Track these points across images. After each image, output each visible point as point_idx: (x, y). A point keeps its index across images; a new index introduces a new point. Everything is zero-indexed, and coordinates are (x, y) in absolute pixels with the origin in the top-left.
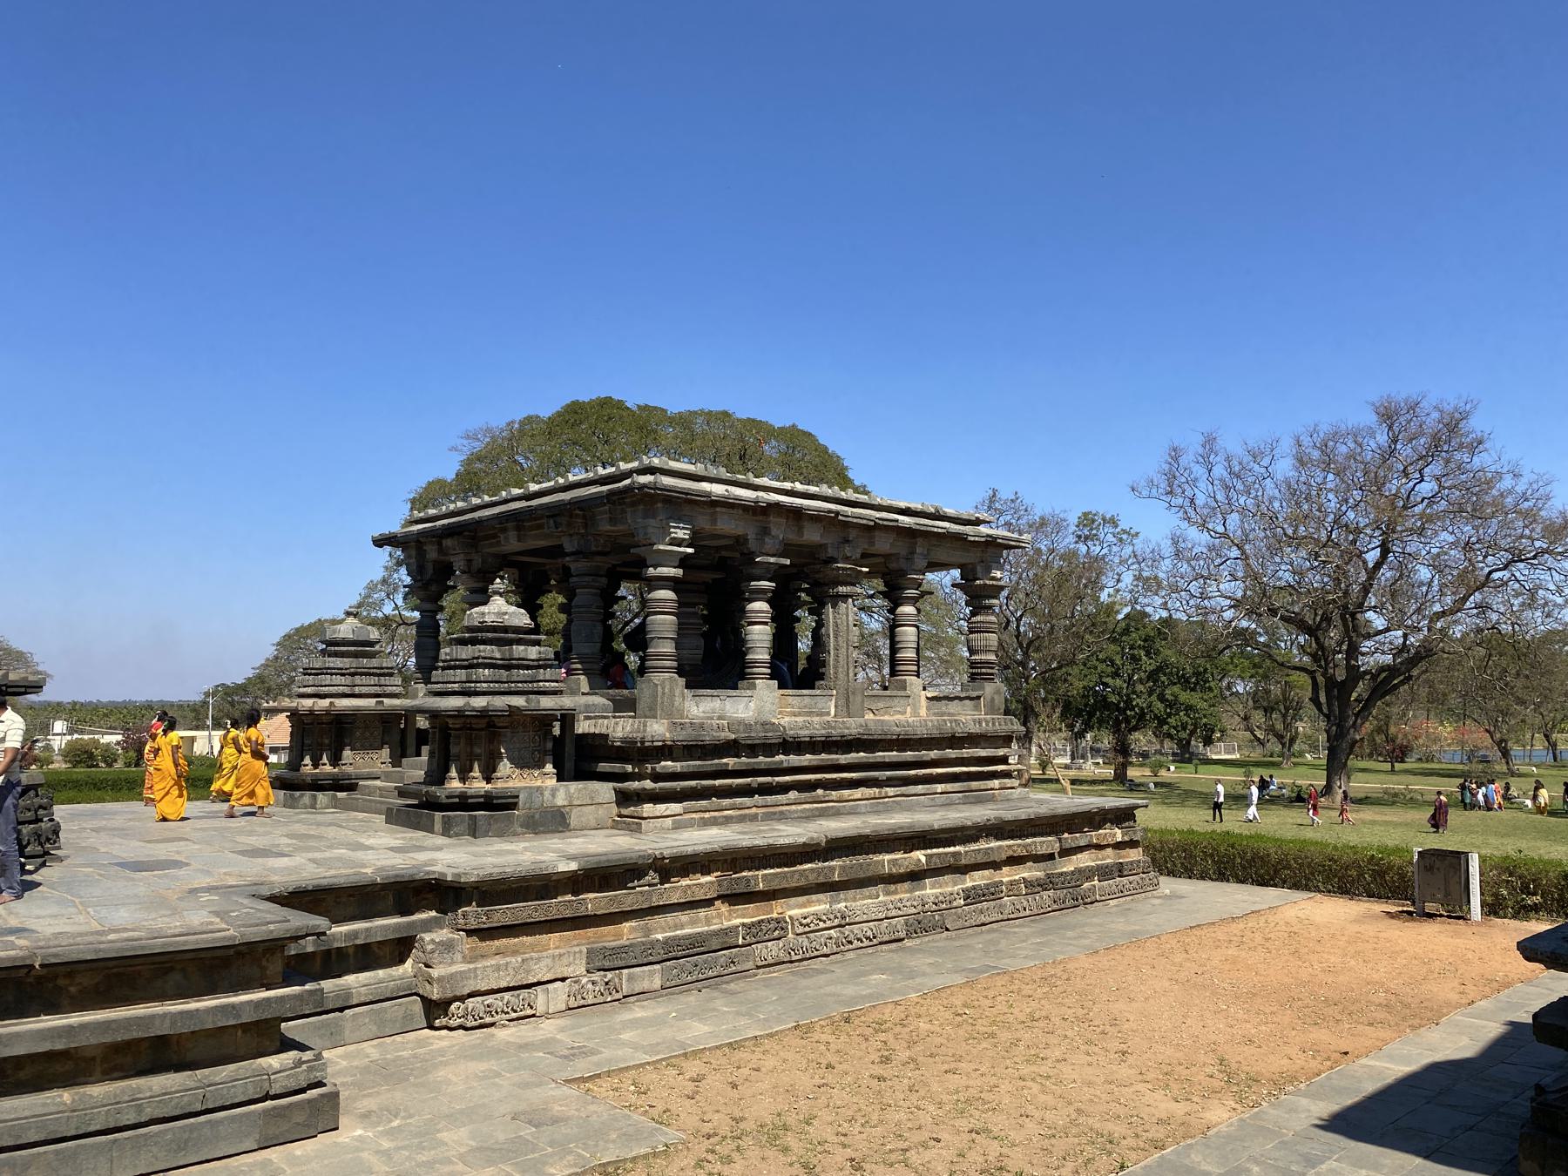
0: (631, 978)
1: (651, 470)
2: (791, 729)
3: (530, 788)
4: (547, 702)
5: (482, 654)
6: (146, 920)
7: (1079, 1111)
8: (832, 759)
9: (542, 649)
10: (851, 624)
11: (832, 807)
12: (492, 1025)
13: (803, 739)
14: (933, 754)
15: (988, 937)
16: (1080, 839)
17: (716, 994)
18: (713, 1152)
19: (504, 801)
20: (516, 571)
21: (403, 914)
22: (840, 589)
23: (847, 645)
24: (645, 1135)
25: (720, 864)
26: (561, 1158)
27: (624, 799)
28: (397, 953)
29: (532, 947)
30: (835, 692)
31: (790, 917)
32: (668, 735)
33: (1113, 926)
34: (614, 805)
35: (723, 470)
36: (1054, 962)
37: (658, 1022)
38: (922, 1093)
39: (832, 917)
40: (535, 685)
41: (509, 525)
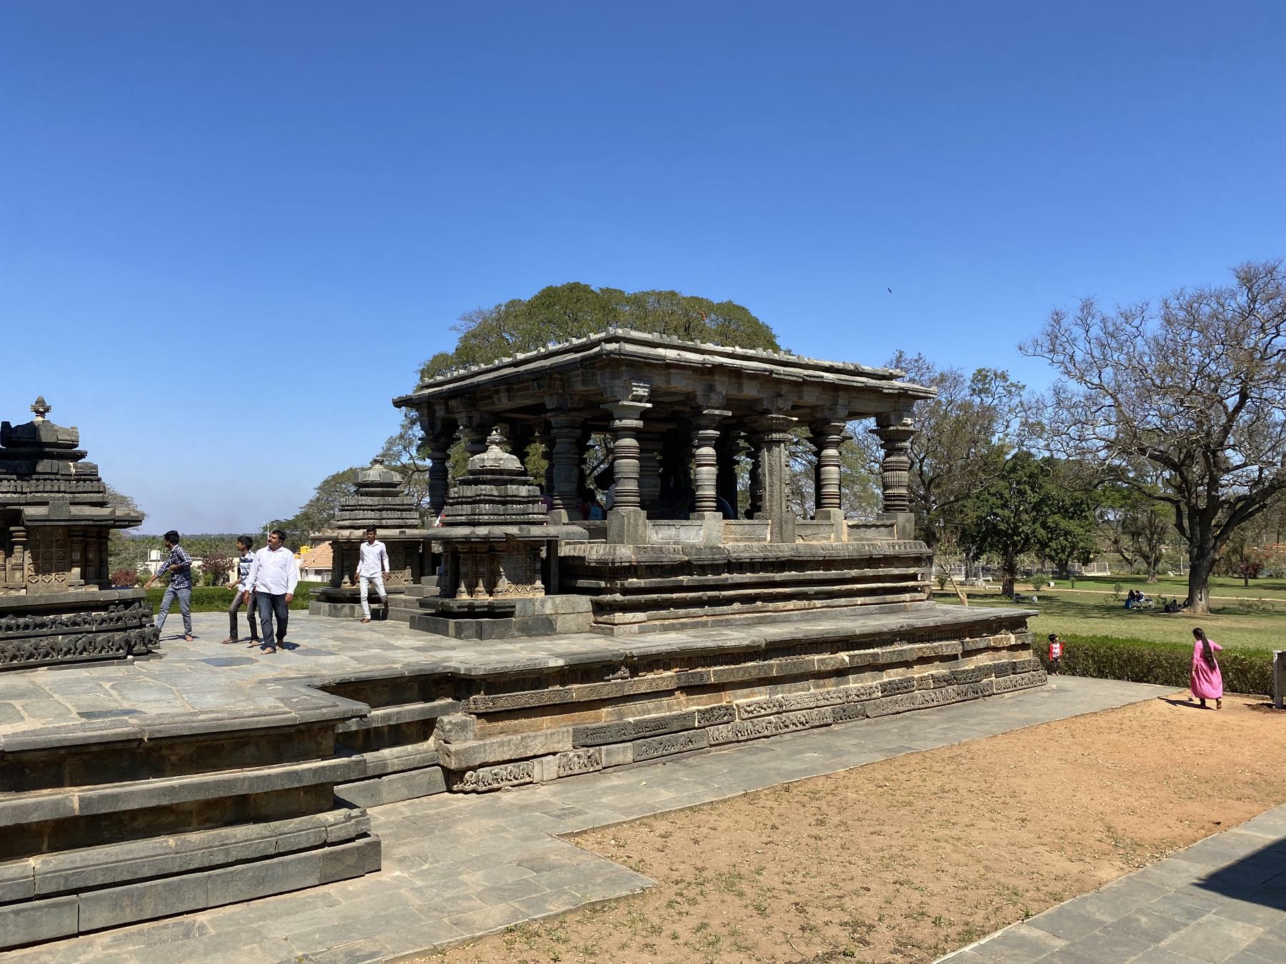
0: (608, 753)
1: (616, 339)
2: (735, 552)
3: (525, 599)
4: (536, 531)
6: (228, 704)
7: (986, 868)
8: (769, 577)
9: (531, 488)
10: (783, 464)
11: (769, 616)
12: (498, 790)
13: (744, 561)
14: (854, 573)
15: (902, 723)
16: (980, 642)
17: (677, 767)
18: (681, 895)
19: (503, 610)
21: (426, 701)
22: (774, 435)
24: (625, 880)
25: (678, 662)
26: (558, 897)
27: (599, 608)
28: (422, 732)
31: (737, 705)
32: (633, 557)
33: (1009, 714)
34: (591, 613)
35: (675, 337)
37: (629, 789)
38: (853, 850)
39: (771, 706)
40: (526, 517)
41: (502, 387)
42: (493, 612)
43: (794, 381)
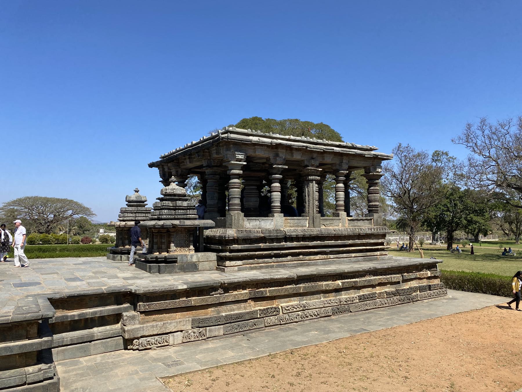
3: (182, 255)
5: (165, 204)
8: (306, 244)
11: (306, 262)
12: (150, 349)
13: (293, 236)
14: (350, 242)
15: (368, 315)
16: (412, 275)
19: (171, 260)
20: (199, 175)
21: (118, 304)
22: (310, 177)
23: (313, 199)
28: (116, 320)
29: (169, 318)
30: (308, 218)
33: (423, 312)
35: (259, 131)
36: (391, 328)
37: (214, 350)
39: (299, 307)
40: (185, 216)
42: (166, 261)
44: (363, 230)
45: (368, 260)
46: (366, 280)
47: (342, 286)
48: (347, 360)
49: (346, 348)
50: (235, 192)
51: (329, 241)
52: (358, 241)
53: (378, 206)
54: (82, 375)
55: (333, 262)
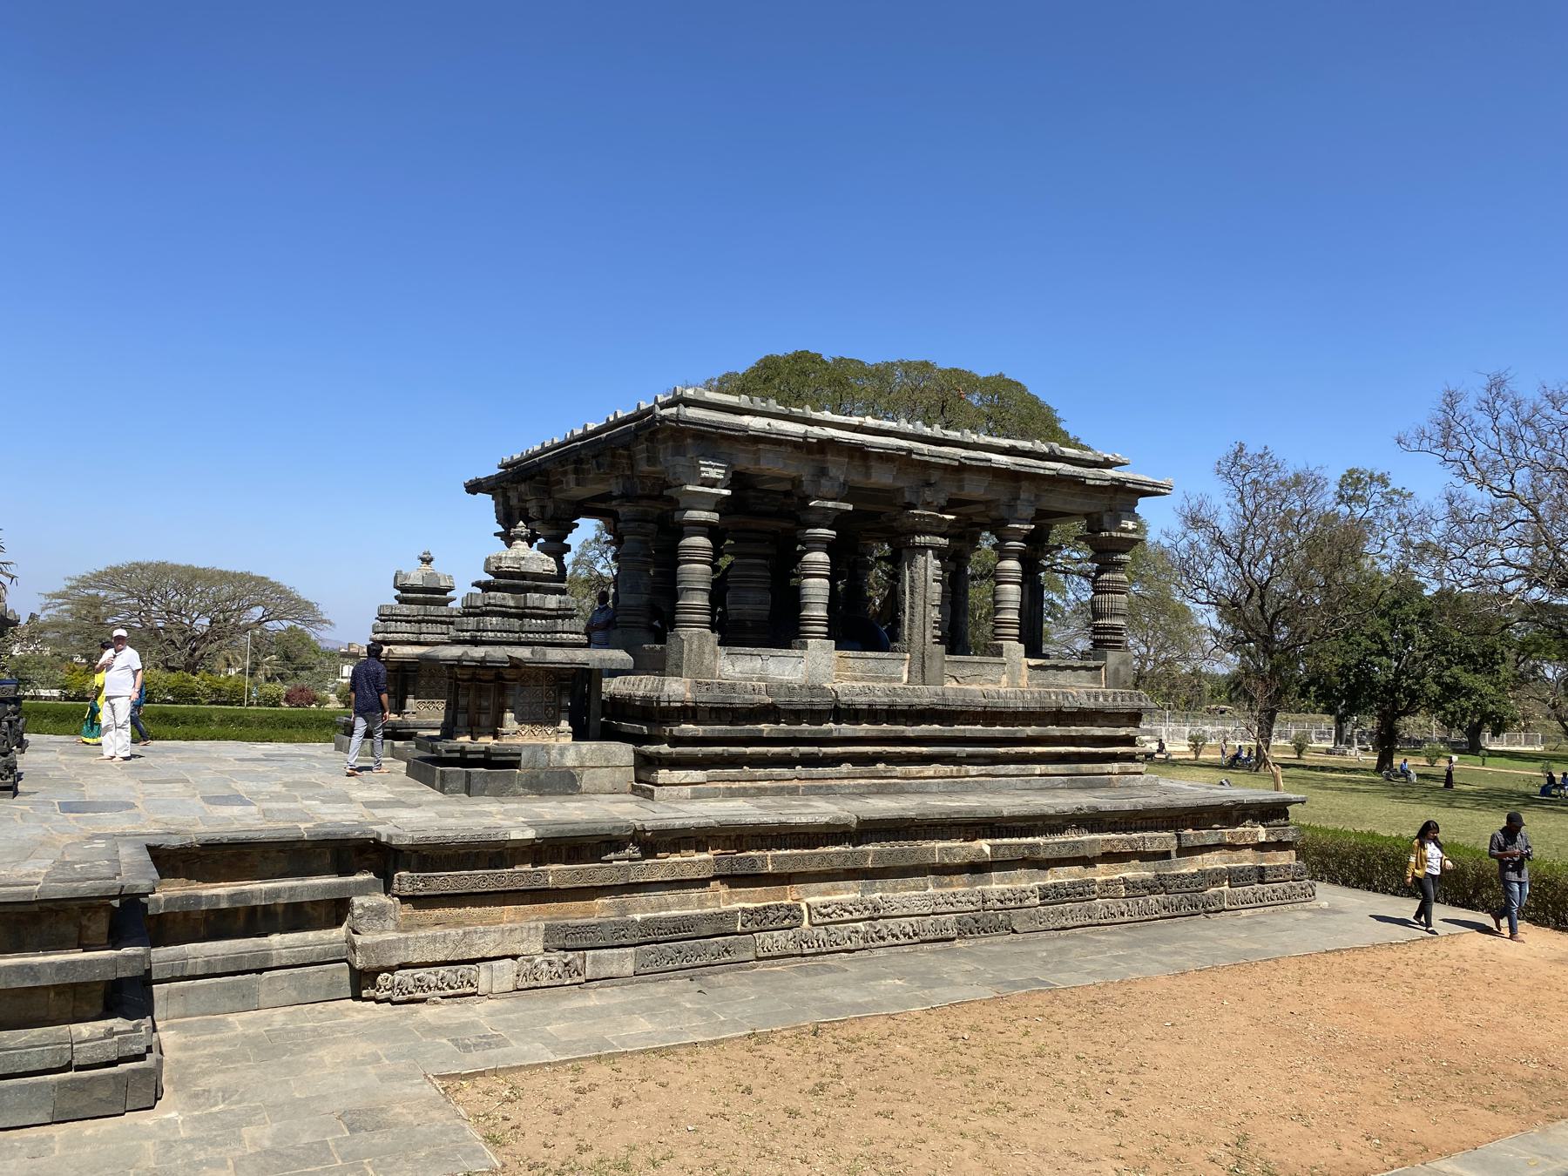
3: (535, 745)
5: (492, 601)
8: (896, 731)
9: (563, 598)
10: (930, 579)
11: (895, 784)
12: (423, 1000)
13: (858, 707)
14: (1032, 730)
15: (1060, 943)
16: (1208, 836)
19: (504, 758)
20: (611, 520)
30: (908, 656)
33: (1228, 942)
35: (772, 402)
36: (1120, 982)
37: (602, 1013)
39: (861, 907)
40: (548, 636)
42: (489, 760)
43: (945, 465)
44: (1070, 698)
45: (1082, 785)
46: (1064, 843)
47: (992, 856)
48: (965, 1060)
49: (972, 1028)
50: (696, 574)
51: (968, 724)
52: (1053, 730)
53: (1121, 629)
54: (226, 1058)
55: (976, 785)
